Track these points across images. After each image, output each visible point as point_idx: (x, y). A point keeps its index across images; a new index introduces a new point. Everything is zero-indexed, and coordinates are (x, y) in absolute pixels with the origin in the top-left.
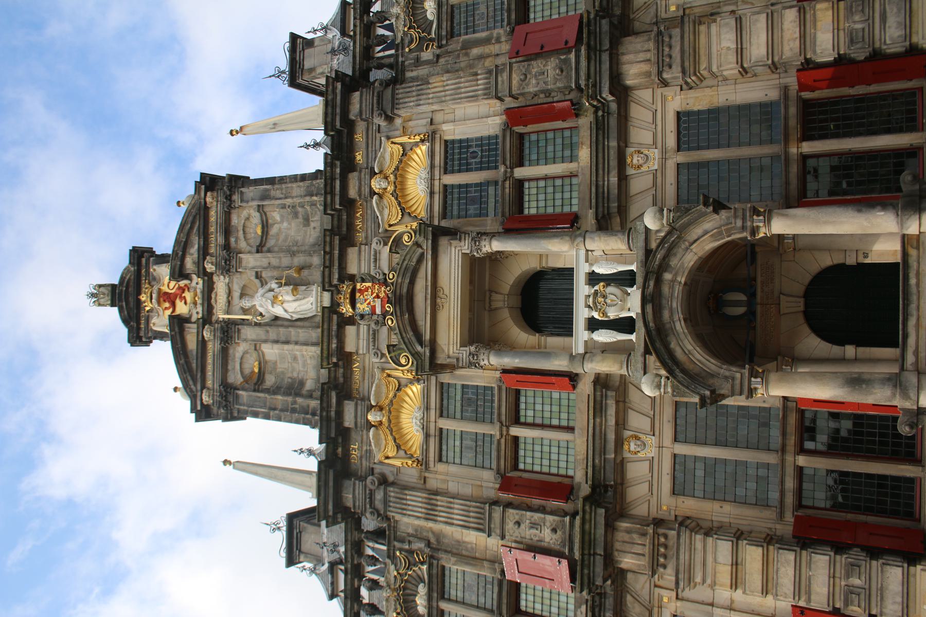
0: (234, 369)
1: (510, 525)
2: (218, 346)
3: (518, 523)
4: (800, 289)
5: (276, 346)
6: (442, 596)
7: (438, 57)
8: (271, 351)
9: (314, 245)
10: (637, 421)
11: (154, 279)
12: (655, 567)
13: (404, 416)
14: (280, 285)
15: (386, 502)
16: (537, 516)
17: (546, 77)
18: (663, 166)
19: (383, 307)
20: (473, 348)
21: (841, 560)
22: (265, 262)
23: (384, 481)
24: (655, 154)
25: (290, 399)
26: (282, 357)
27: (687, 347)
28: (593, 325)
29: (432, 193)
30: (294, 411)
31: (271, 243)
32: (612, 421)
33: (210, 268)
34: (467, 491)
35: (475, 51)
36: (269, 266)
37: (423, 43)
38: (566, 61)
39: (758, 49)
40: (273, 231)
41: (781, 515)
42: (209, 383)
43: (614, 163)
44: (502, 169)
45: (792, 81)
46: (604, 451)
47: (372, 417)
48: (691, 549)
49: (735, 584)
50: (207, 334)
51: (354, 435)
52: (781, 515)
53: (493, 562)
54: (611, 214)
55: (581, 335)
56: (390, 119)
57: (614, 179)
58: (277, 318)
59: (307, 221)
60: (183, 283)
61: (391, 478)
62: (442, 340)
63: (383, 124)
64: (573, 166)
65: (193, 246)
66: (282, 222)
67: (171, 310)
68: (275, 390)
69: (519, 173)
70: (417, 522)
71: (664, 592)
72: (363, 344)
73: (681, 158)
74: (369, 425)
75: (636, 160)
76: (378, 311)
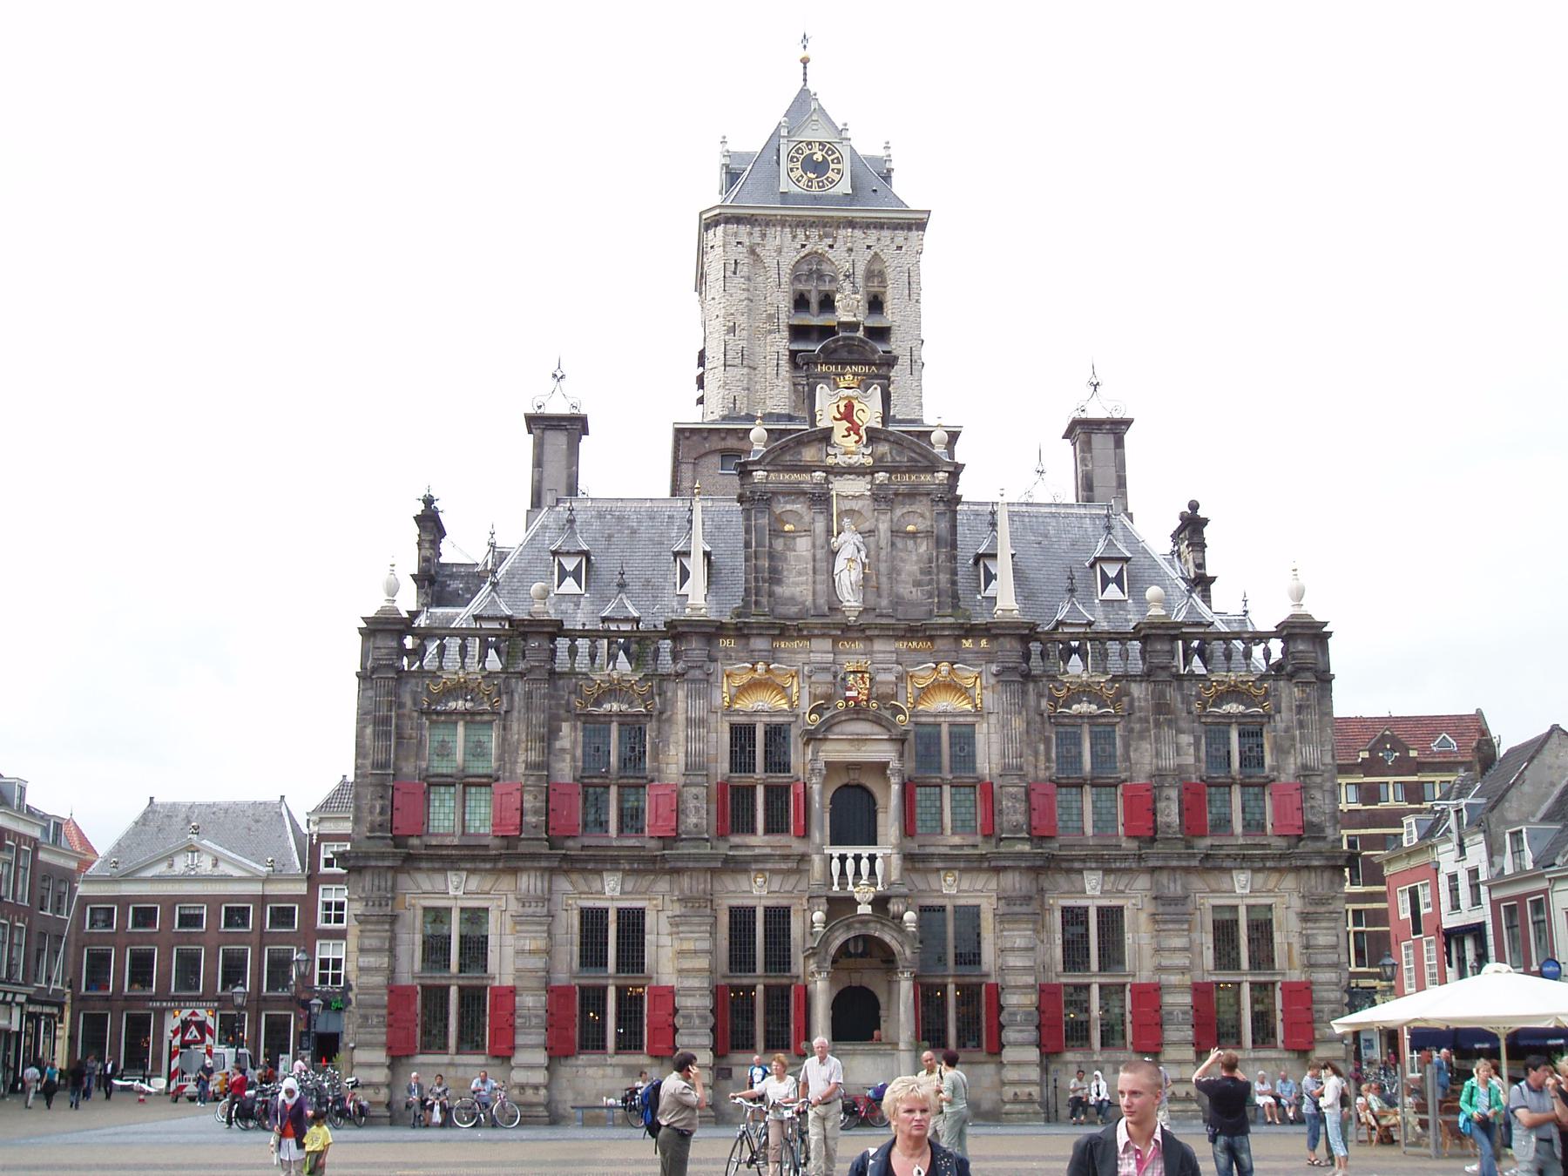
1: (694, 790)
5: (808, 555)
8: (803, 544)
9: (898, 596)
12: (683, 900)
14: (864, 564)
15: (693, 681)
17: (1013, 812)
18: (945, 896)
21: (708, 1013)
22: (883, 543)
26: (798, 558)
28: (843, 858)
32: (777, 866)
33: (881, 476)
35: (1042, 747)
37: (1054, 700)
38: (1021, 830)
39: (1014, 961)
40: (910, 543)
41: (724, 977)
44: (950, 777)
45: (992, 980)
48: (700, 925)
49: (681, 953)
50: (819, 475)
51: (743, 641)
52: (724, 977)
53: (658, 770)
54: (913, 861)
55: (836, 851)
57: (940, 865)
58: (834, 554)
59: (917, 584)
61: (712, 679)
62: (828, 746)
63: (994, 668)
64: (948, 831)
65: (900, 453)
68: (772, 556)
69: (946, 788)
70: (681, 705)
71: (659, 902)
73: (949, 908)
75: (950, 879)
76: (848, 694)
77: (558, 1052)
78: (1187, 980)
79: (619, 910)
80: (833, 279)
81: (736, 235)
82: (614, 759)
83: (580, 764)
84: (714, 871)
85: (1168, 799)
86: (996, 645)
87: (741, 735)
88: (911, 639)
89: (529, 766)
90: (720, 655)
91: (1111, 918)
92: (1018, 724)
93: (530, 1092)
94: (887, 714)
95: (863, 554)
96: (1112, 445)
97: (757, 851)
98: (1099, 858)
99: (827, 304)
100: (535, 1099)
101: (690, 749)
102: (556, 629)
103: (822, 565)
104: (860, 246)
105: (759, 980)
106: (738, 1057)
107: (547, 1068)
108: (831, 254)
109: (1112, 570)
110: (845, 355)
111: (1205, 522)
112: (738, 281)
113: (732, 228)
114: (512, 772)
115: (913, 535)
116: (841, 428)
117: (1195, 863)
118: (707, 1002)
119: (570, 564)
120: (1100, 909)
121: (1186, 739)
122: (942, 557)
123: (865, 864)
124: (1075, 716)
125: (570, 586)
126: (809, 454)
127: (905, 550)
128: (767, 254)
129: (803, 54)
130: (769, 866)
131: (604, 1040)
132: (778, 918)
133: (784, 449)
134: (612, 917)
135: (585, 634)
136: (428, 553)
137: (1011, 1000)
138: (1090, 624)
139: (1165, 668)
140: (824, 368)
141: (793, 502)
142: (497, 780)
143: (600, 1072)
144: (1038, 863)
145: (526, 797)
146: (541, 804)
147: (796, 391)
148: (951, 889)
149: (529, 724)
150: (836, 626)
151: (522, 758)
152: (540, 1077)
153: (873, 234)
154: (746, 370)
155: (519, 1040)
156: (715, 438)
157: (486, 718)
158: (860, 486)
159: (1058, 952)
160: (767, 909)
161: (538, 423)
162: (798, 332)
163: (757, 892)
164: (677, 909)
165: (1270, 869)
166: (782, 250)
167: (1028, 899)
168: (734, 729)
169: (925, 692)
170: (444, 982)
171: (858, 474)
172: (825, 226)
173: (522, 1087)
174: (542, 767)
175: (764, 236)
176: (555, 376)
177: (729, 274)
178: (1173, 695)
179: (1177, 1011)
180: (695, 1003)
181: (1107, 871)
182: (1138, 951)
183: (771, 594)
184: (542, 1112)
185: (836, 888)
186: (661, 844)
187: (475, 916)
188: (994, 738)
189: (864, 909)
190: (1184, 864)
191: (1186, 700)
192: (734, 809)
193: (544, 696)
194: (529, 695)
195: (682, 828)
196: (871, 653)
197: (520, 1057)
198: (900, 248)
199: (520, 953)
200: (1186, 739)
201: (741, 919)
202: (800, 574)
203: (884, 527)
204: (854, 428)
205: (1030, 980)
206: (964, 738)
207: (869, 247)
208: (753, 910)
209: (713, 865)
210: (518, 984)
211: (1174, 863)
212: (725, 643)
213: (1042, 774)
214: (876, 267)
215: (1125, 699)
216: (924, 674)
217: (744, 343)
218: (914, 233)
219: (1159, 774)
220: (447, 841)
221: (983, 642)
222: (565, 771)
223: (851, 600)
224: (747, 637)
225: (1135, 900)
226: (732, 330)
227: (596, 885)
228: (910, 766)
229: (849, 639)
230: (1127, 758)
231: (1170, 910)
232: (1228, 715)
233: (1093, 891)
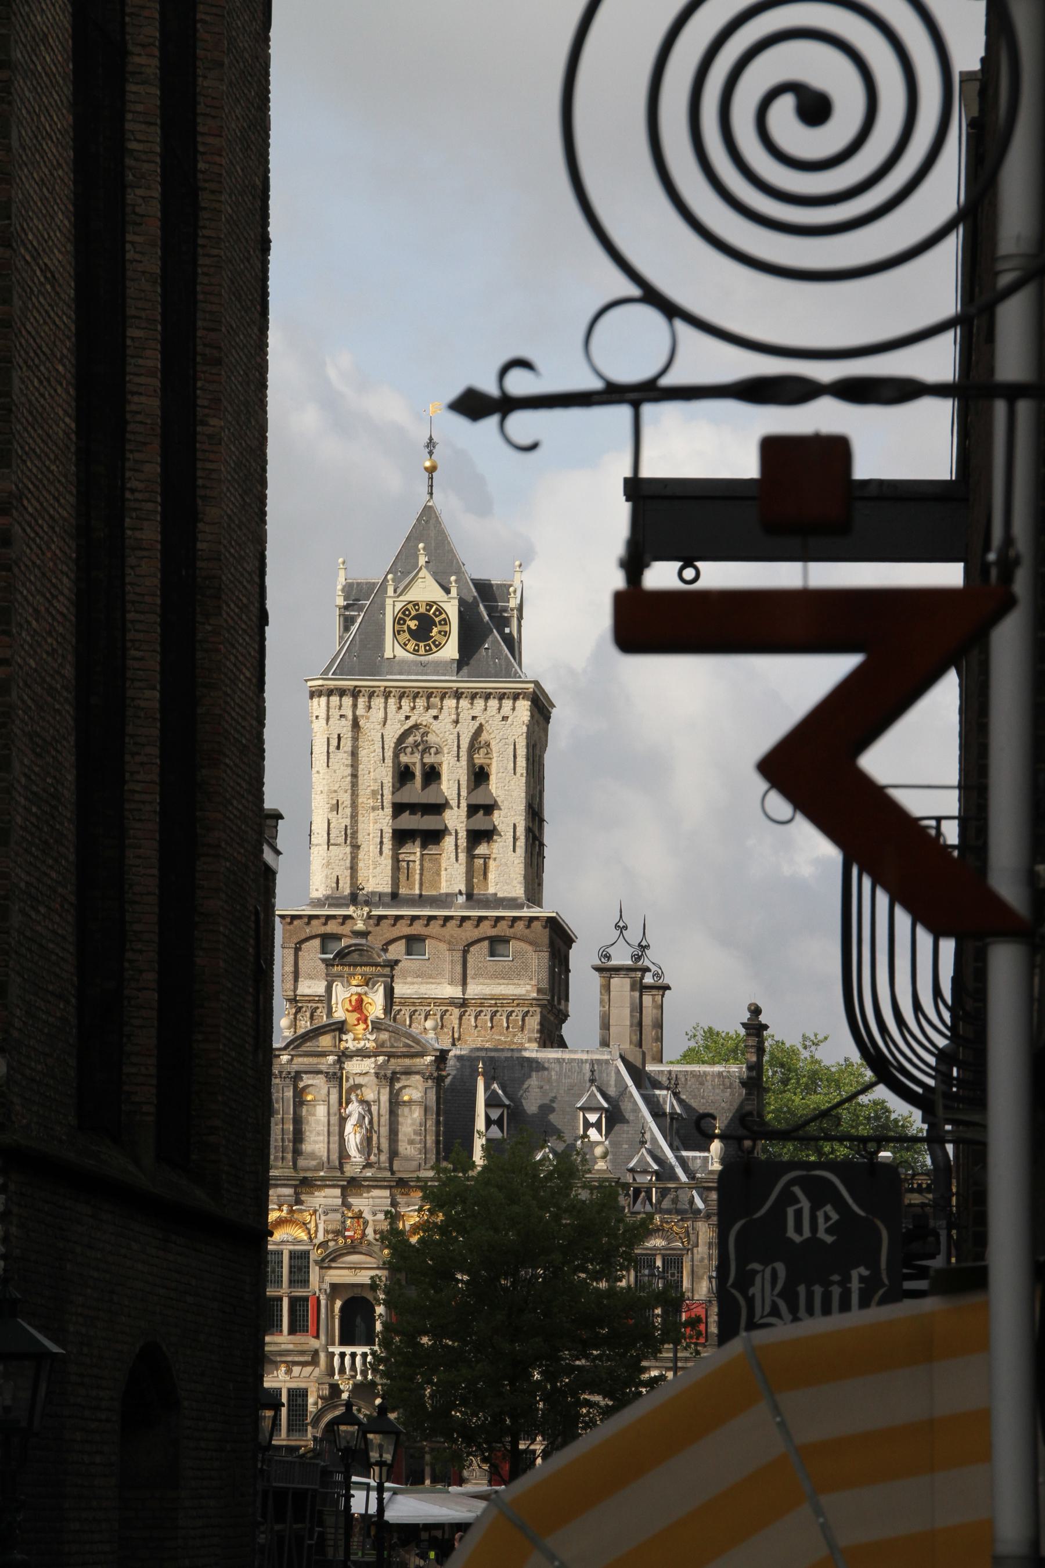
8: (321, 1111)
19: (349, 1237)
20: (328, 1291)
25: (291, 1136)
26: (318, 1122)
28: (342, 1355)
30: (283, 1140)
32: (296, 1359)
46: (281, 1355)
47: (285, 1208)
55: (337, 1350)
59: (411, 1142)
62: (332, 1272)
67: (350, 1008)
68: (298, 1121)
72: (330, 1201)
76: (347, 1234)
97: (283, 1347)
99: (432, 775)
103: (335, 1129)
104: (465, 716)
108: (435, 725)
113: (335, 700)
115: (410, 1102)
116: (352, 1018)
126: (325, 1041)
128: (371, 725)
129: (428, 464)
140: (339, 968)
141: (314, 1078)
162: (398, 809)
171: (365, 1057)
177: (332, 749)
198: (505, 718)
202: (318, 1134)
207: (474, 718)
226: (336, 807)
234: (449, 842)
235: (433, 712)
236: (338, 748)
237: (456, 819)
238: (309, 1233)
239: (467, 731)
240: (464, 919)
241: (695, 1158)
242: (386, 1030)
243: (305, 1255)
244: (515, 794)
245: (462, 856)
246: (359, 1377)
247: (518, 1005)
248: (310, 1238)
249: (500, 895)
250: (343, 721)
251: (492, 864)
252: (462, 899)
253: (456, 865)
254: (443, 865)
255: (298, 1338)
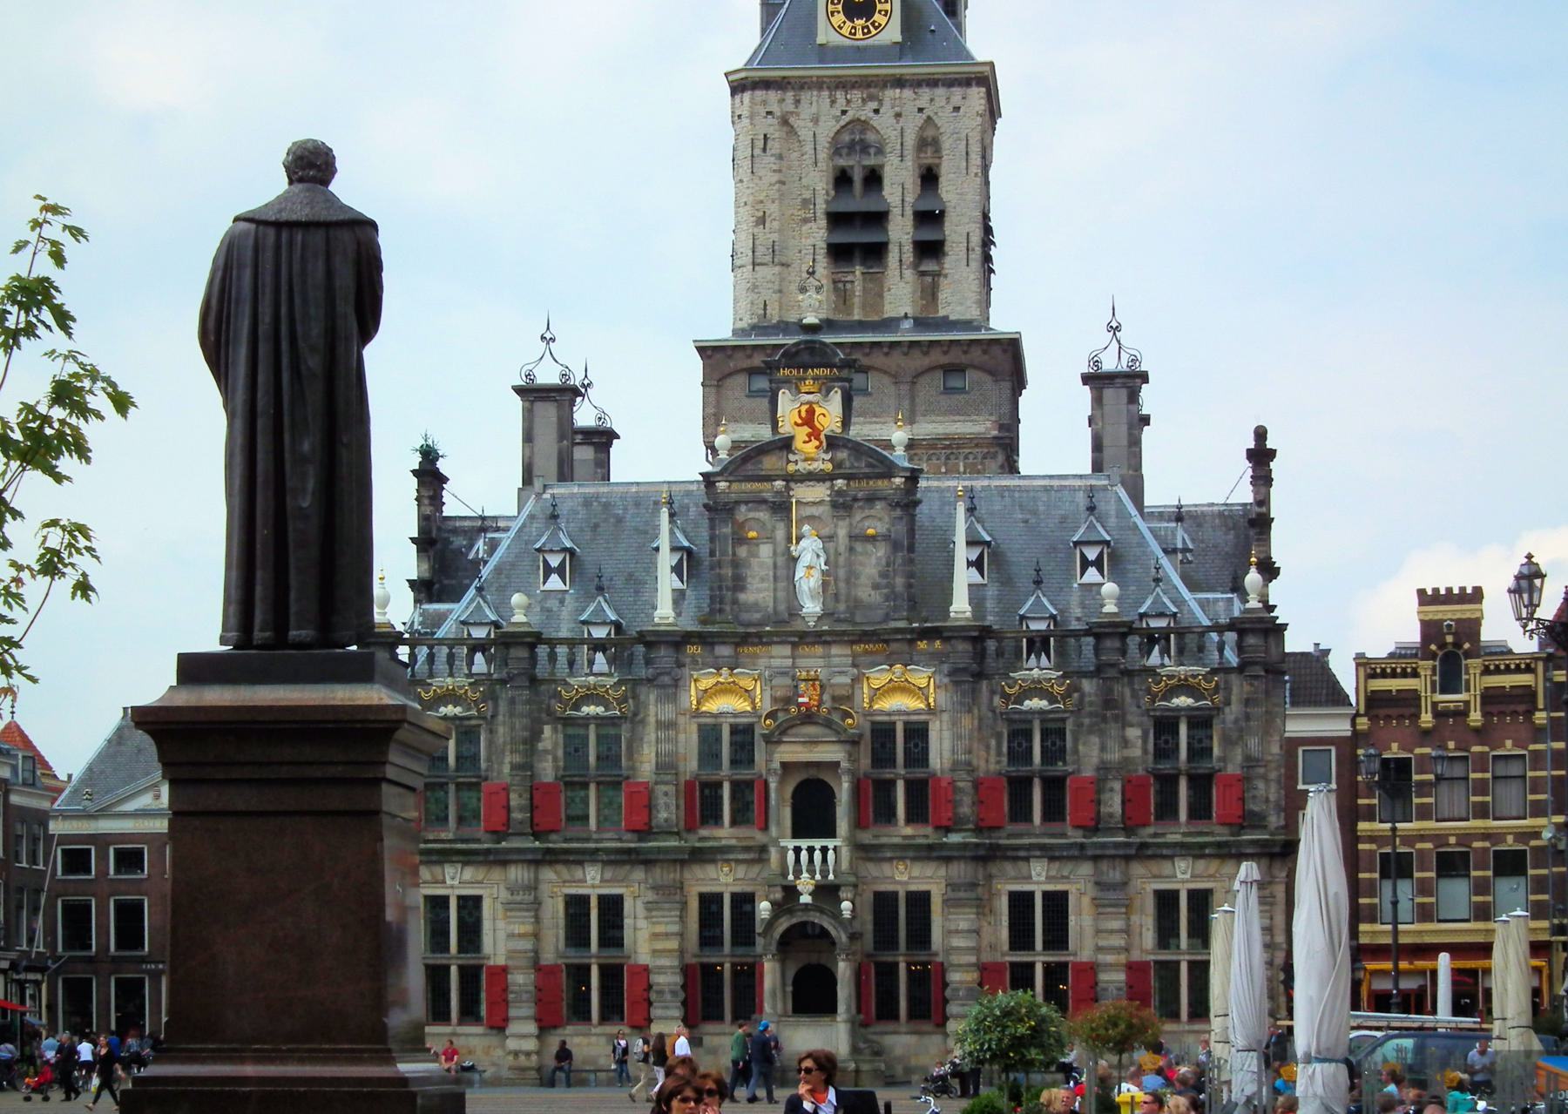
0: (750, 510)
1: (664, 788)
2: (768, 496)
3: (666, 794)
4: (823, 962)
5: (770, 562)
6: (597, 726)
7: (993, 711)
8: (765, 551)
10: (741, 871)
11: (828, 392)
13: (725, 695)
15: (664, 687)
16: (673, 808)
22: (842, 549)
23: (676, 684)
24: (905, 878)
25: (730, 584)
26: (761, 565)
27: (784, 924)
28: (797, 850)
29: (889, 714)
31: (859, 547)
32: (741, 857)
33: (840, 483)
34: (681, 750)
35: (993, 743)
36: (838, 554)
37: (1006, 697)
38: (968, 822)
39: (957, 942)
40: (869, 547)
41: (695, 956)
42: (735, 486)
43: (898, 854)
45: (939, 959)
48: (670, 910)
49: (655, 936)
50: (779, 484)
52: (695, 956)
53: (633, 768)
55: (791, 844)
56: (949, 675)
57: (889, 855)
58: (795, 560)
59: (876, 587)
60: (822, 437)
62: (783, 748)
63: (946, 668)
66: (879, 559)
68: (736, 564)
70: (652, 709)
72: (776, 662)
74: (718, 669)
77: (546, 1023)
78: (1122, 958)
79: (601, 898)
80: (880, 151)
81: (764, 103)
82: (592, 759)
83: (561, 764)
84: (683, 863)
85: (1112, 790)
86: (948, 648)
87: (709, 734)
88: (868, 642)
89: (514, 767)
90: (688, 660)
91: (1057, 904)
92: (967, 722)
93: (522, 1058)
94: (836, 717)
95: (822, 560)
96: (1125, 400)
97: (724, 842)
98: (1042, 847)
99: (874, 179)
100: (527, 1064)
101: (662, 748)
102: (532, 640)
103: (782, 573)
104: (910, 109)
105: (725, 958)
106: (709, 1027)
107: (538, 1037)
108: (876, 121)
109: (1092, 554)
110: (806, 357)
111: (1272, 454)
112: (769, 161)
113: (760, 94)
114: (500, 772)
115: (872, 539)
116: (802, 433)
117: (1133, 852)
118: (678, 979)
119: (554, 561)
120: (1046, 894)
121: (1133, 733)
122: (899, 561)
123: (818, 855)
124: (1026, 712)
125: (555, 582)
126: (770, 463)
127: (866, 553)
130: (731, 856)
131: (589, 1012)
132: (744, 902)
133: (746, 459)
134: (594, 903)
135: (562, 641)
136: (428, 510)
137: (954, 977)
138: (1053, 617)
139: (1112, 665)
140: (787, 372)
142: (486, 779)
143: (584, 1040)
144: (982, 852)
145: (513, 796)
146: (525, 802)
147: (836, 289)
148: (904, 877)
149: (513, 728)
150: (793, 634)
151: (507, 759)
152: (531, 1045)
153: (926, 93)
154: (777, 269)
155: (512, 1012)
156: (739, 355)
157: (473, 722)
158: (820, 492)
159: (1004, 934)
160: (734, 896)
161: (531, 393)
162: (837, 220)
163: (724, 880)
164: (651, 896)
165: (1210, 856)
166: (820, 118)
167: (973, 885)
168: (700, 726)
169: (876, 693)
170: (444, 962)
171: (818, 481)
172: (869, 86)
173: (516, 1054)
174: (526, 768)
175: (797, 102)
176: (543, 338)
178: (1123, 691)
179: (1111, 987)
180: (667, 979)
181: (1052, 859)
182: (1081, 933)
183: (735, 602)
184: (533, 1074)
185: (791, 877)
186: (635, 836)
187: (471, 905)
188: (946, 734)
189: (805, 899)
190: (1121, 852)
191: (1134, 695)
192: (702, 803)
193: (528, 702)
194: (512, 702)
195: (653, 823)
196: (829, 657)
197: (513, 1028)
198: (957, 109)
199: (511, 936)
200: (1133, 733)
201: (709, 903)
202: (762, 580)
203: (842, 533)
204: (815, 434)
205: (973, 959)
206: (917, 733)
207: (921, 110)
208: (720, 896)
209: (680, 857)
210: (510, 963)
211: (1112, 852)
212: (691, 649)
213: (993, 767)
214: (930, 133)
215: (1076, 695)
216: (879, 677)
217: (775, 237)
218: (977, 95)
219: (1104, 768)
220: (443, 836)
221: (938, 642)
222: (547, 771)
223: (811, 607)
224: (712, 644)
225: (1078, 884)
226: (762, 221)
227: (578, 874)
228: (865, 762)
229: (807, 644)
230: (1076, 751)
231: (1111, 896)
232: (1178, 709)
233: (1039, 878)
234: (893, 257)
235: (874, 105)
236: (764, 150)
237: (901, 231)
238: (753, 703)
239: (912, 124)
240: (912, 344)
241: (1217, 600)
242: (845, 446)
243: (749, 729)
244: (969, 197)
245: (909, 274)
246: (818, 877)
247: (977, 446)
248: (754, 708)
249: (952, 318)
250: (770, 119)
251: (943, 282)
252: (907, 324)
253: (902, 284)
254: (886, 285)
255: (742, 832)
